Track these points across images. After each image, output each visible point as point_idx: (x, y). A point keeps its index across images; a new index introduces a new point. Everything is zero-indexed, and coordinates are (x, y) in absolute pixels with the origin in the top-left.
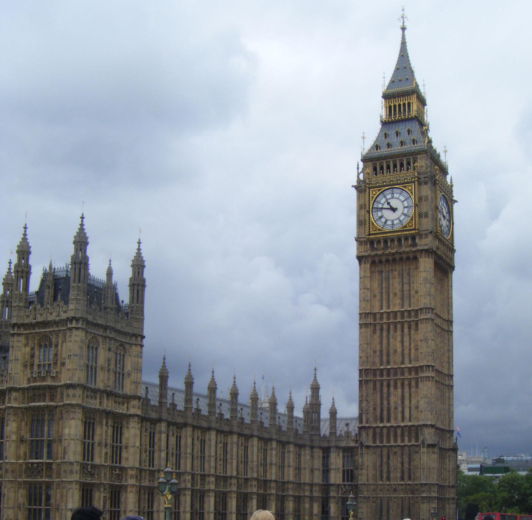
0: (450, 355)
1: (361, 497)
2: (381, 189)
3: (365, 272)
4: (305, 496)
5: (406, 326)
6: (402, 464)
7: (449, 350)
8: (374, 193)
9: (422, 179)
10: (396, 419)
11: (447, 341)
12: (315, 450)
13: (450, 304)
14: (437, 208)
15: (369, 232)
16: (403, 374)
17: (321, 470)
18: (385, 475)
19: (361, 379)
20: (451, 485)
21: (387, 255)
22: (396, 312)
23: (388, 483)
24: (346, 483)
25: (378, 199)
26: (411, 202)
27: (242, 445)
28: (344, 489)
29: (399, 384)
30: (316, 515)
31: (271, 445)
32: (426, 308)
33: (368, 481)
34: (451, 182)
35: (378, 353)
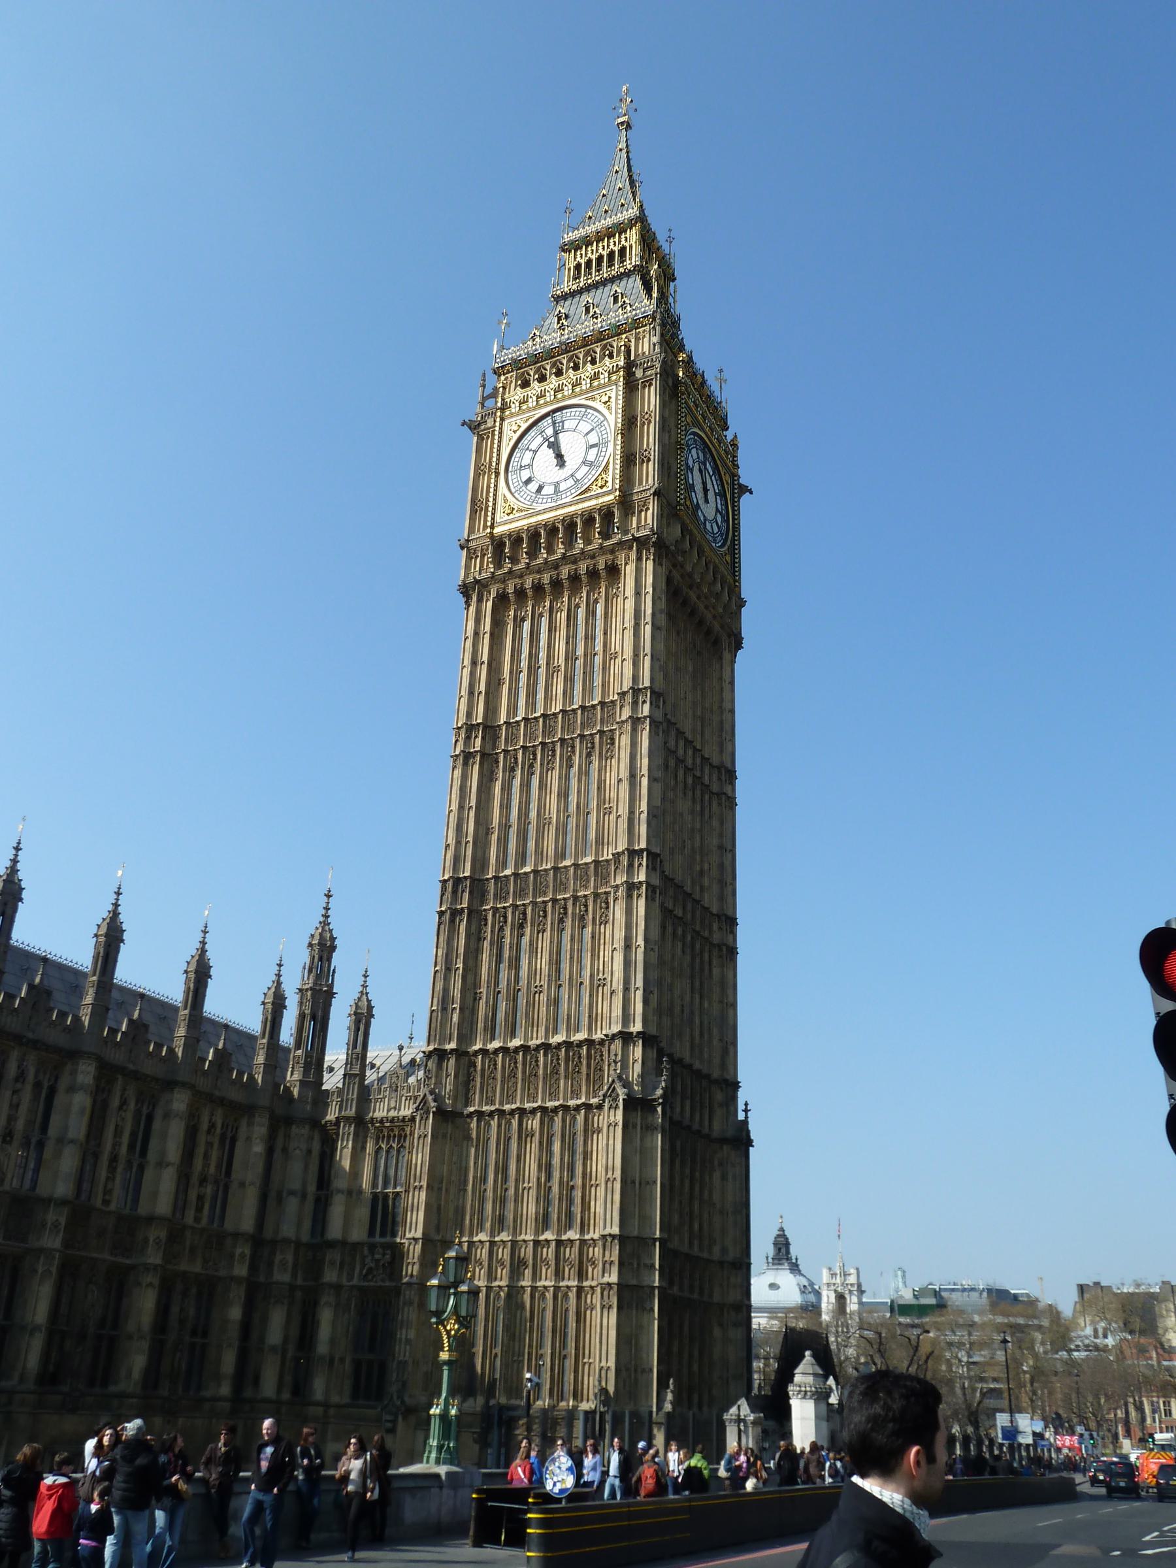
0: (727, 863)
3: (478, 621)
4: (232, 1278)
8: (515, 428)
9: (639, 373)
11: (715, 823)
12: (294, 1130)
13: (727, 726)
17: (311, 1198)
24: (378, 1239)
25: (525, 441)
28: (368, 1260)
30: (273, 1349)
31: (74, 1073)
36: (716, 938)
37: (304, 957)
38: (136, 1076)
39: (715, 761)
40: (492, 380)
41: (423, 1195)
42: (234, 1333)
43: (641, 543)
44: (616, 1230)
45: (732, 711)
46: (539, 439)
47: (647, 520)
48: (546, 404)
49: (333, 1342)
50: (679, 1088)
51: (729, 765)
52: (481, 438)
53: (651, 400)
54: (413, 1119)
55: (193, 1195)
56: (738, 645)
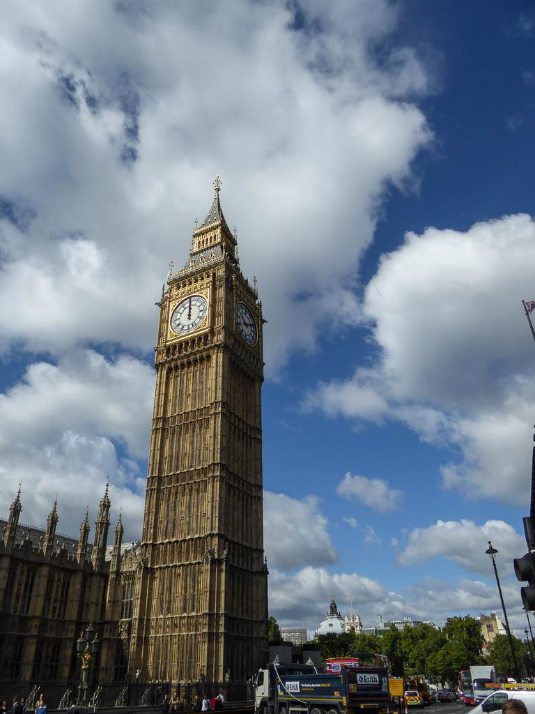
5: (197, 426)
6: (186, 589)
16: (191, 478)
20: (260, 619)
22: (188, 412)
23: (169, 616)
29: (187, 491)
32: (216, 403)
36: (254, 494)
37: (98, 509)
38: (28, 562)
39: (253, 425)
40: (167, 287)
41: (139, 601)
42: (68, 661)
43: (218, 346)
44: (207, 611)
45: (260, 406)
46: (183, 309)
47: (220, 338)
48: (185, 295)
49: (107, 662)
50: (236, 553)
51: (259, 427)
52: (162, 309)
53: (221, 293)
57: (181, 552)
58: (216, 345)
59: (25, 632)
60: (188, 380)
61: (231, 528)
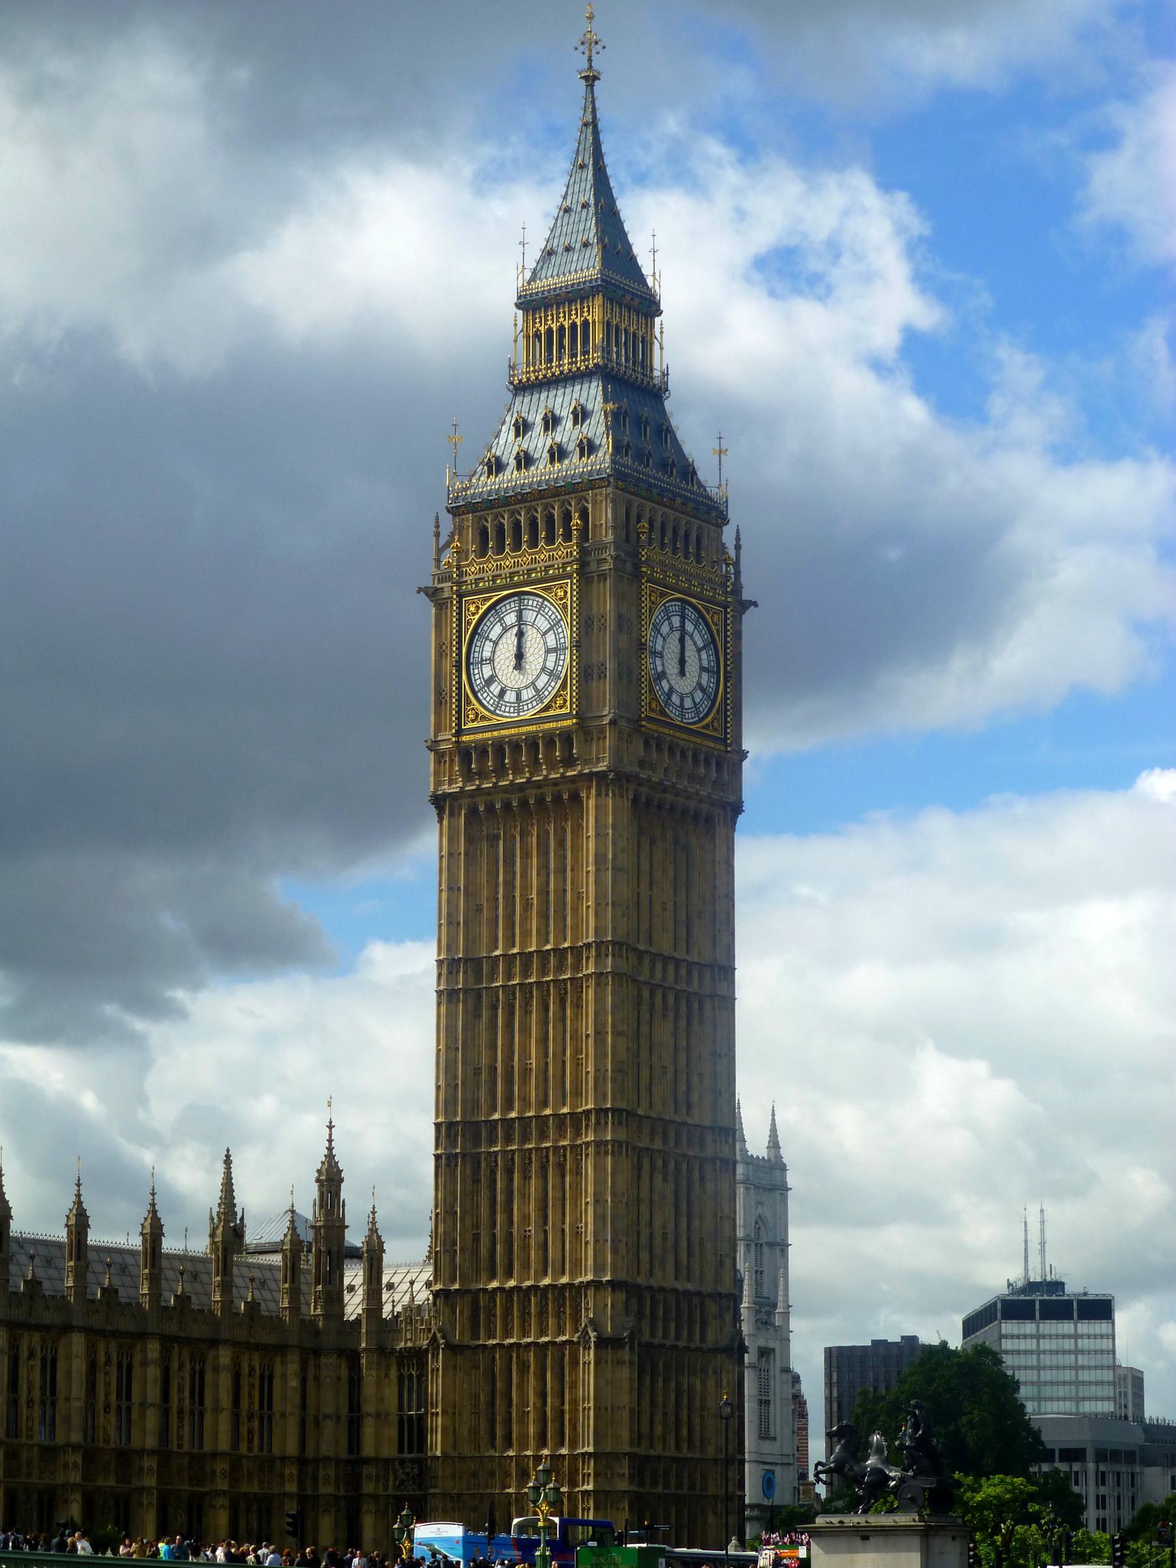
1: (434, 1494)
2: (490, 598)
4: (285, 1494)
6: (543, 1395)
7: (714, 1054)
9: (593, 566)
10: (526, 1265)
14: (642, 647)
15: (459, 725)
17: (344, 1420)
18: (499, 1431)
19: (439, 1152)
21: (505, 789)
24: (406, 1455)
26: (566, 634)
27: (31, 1355)
28: (399, 1473)
31: (144, 1351)
33: (455, 1447)
34: (738, 547)
35: (484, 1076)
37: (313, 1192)
38: (188, 1341)
40: (448, 523)
43: (601, 776)
44: (591, 1449)
46: (498, 629)
52: (441, 605)
54: (427, 1350)
55: (244, 1430)
56: (737, 808)
57: (529, 1314)
58: (591, 773)
59: (202, 1486)
60: (526, 855)
61: (644, 1255)
